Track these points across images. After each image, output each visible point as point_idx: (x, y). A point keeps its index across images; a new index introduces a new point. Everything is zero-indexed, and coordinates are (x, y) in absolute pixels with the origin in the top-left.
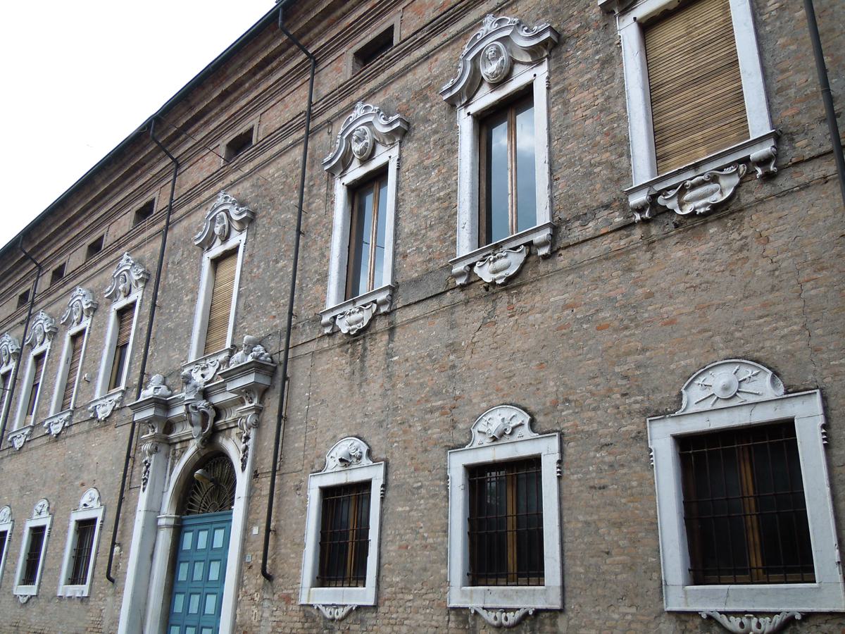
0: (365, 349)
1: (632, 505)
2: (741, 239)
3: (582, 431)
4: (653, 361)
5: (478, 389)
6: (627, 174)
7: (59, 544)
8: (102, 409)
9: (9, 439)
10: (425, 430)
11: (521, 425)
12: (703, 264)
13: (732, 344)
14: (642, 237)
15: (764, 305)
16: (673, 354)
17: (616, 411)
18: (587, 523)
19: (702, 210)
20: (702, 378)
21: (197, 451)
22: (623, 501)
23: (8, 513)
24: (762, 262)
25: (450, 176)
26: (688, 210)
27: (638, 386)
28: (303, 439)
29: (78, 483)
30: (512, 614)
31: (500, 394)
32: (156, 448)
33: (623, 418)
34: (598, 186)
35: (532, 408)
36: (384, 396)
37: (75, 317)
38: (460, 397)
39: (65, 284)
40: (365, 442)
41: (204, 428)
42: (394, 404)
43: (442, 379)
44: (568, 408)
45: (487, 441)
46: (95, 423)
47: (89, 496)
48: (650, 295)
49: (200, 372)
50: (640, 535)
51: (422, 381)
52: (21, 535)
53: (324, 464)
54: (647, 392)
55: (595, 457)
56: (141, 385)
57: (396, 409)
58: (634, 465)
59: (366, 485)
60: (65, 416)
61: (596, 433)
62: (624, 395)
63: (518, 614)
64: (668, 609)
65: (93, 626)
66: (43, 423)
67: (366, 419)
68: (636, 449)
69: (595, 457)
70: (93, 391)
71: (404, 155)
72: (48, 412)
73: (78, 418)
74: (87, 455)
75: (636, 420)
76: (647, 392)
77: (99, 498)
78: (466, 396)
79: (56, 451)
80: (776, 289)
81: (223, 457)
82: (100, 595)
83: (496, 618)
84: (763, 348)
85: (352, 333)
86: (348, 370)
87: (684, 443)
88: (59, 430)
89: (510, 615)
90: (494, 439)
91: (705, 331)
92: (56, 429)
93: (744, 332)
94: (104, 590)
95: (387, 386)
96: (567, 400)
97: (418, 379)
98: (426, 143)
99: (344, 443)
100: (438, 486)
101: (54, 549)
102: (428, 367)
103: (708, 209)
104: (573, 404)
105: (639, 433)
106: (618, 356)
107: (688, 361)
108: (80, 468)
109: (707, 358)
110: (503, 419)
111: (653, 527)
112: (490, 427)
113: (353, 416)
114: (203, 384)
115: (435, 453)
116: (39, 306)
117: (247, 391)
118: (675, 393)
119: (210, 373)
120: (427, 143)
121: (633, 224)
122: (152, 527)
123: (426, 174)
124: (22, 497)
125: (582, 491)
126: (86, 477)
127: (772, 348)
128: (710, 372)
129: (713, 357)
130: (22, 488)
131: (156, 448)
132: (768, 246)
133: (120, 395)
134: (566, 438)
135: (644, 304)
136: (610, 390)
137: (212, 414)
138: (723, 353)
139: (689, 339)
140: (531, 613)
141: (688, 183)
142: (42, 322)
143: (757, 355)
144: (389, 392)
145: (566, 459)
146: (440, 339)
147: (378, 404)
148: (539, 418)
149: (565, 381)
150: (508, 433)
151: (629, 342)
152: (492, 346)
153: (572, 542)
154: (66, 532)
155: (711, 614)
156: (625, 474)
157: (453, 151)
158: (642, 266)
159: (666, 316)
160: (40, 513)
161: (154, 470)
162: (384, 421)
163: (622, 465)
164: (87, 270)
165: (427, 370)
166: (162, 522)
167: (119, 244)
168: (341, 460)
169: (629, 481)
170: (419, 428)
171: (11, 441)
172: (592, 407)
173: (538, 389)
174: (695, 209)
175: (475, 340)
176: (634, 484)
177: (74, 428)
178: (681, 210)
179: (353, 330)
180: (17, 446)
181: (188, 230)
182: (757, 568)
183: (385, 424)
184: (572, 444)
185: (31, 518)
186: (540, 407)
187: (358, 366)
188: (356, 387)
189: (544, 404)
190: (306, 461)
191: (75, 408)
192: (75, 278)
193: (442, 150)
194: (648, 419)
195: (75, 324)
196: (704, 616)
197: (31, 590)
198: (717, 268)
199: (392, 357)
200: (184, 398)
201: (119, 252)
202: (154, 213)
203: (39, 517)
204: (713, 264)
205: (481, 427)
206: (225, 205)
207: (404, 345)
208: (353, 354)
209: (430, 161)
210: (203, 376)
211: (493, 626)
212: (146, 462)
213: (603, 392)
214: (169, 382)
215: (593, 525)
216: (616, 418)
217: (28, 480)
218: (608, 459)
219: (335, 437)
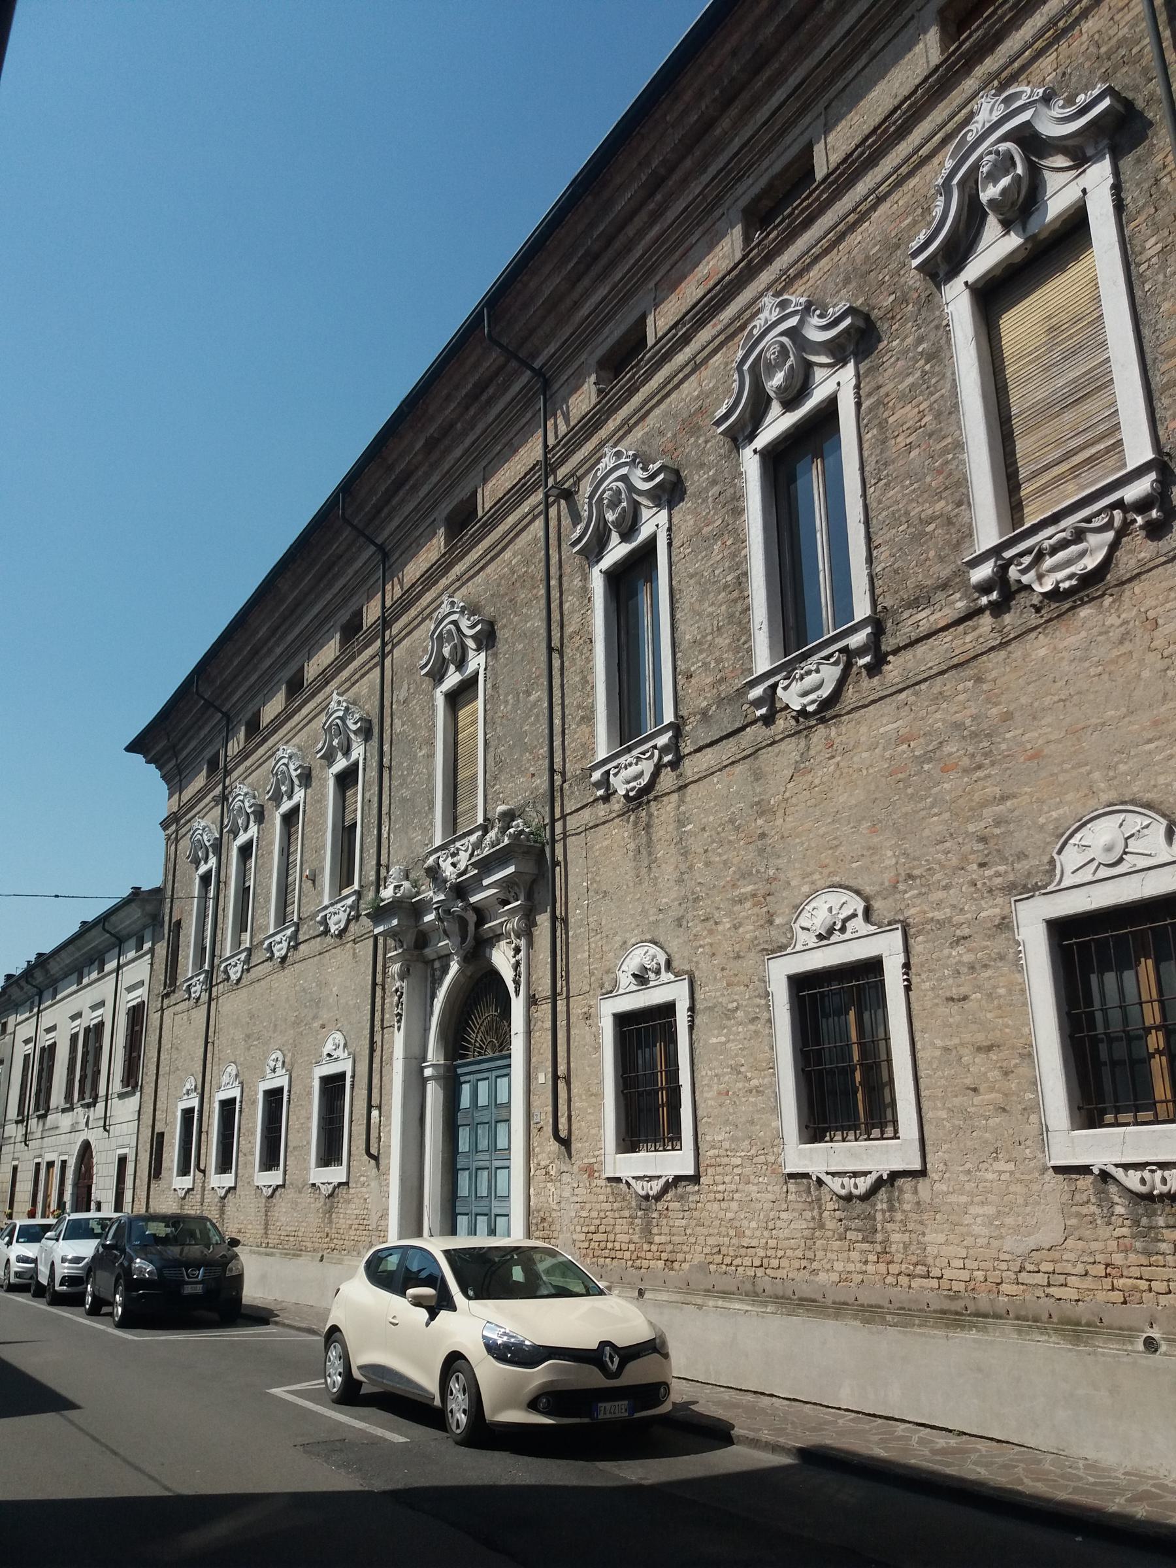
0: (650, 815)
1: (1000, 1021)
2: (1121, 625)
3: (932, 919)
4: (1016, 813)
5: (797, 865)
6: (968, 534)
7: (303, 1112)
8: (335, 919)
9: (222, 968)
10: (736, 927)
11: (854, 915)
12: (1074, 665)
13: (1115, 782)
14: (993, 629)
15: (1156, 723)
16: (1041, 801)
17: (973, 889)
18: (947, 1049)
19: (1066, 585)
20: (1078, 836)
21: (461, 971)
22: (989, 1015)
23: (234, 1073)
24: (1152, 657)
25: (740, 551)
26: (1048, 586)
27: (998, 851)
28: (586, 948)
29: (316, 1025)
30: (863, 1178)
31: (826, 871)
32: (408, 970)
33: (983, 898)
34: (932, 554)
35: (868, 890)
36: (680, 881)
37: (284, 789)
38: (775, 879)
39: (265, 740)
40: (662, 948)
41: (464, 939)
42: (693, 893)
43: (751, 855)
44: (911, 888)
45: (812, 941)
46: (328, 939)
47: (332, 1042)
48: (1008, 717)
49: (450, 860)
50: (1013, 1062)
51: (725, 857)
52: (254, 1102)
53: (616, 983)
54: (1011, 859)
55: (950, 956)
56: (379, 883)
57: (697, 900)
58: (1000, 964)
59: (669, 1009)
60: (289, 932)
61: (950, 922)
62: (982, 865)
63: (870, 1179)
64: (1054, 1163)
65: (357, 1221)
66: (262, 943)
67: (661, 916)
68: (999, 944)
69: (950, 956)
70: (320, 894)
71: (675, 520)
72: (267, 927)
73: (305, 933)
74: (322, 985)
75: (999, 901)
76: (1011, 859)
77: (345, 1046)
78: (782, 876)
79: (284, 979)
80: (1169, 697)
81: (494, 976)
82: (362, 1179)
83: (843, 1186)
84: (1155, 786)
85: (631, 794)
86: (632, 846)
87: (1062, 931)
88: (283, 952)
89: (860, 1181)
90: (820, 937)
91: (1080, 765)
92: (279, 951)
93: (1131, 764)
94: (366, 1171)
95: (683, 868)
96: (910, 876)
97: (720, 855)
98: (703, 501)
99: (637, 952)
100: (758, 1006)
101: (298, 1119)
102: (731, 838)
103: (1074, 582)
104: (918, 881)
105: (1004, 918)
106: (971, 809)
107: (1061, 811)
108: (317, 1003)
109: (1084, 805)
110: (830, 910)
111: (1028, 1055)
112: (815, 921)
113: (644, 912)
114: (454, 876)
115: (752, 959)
116: (235, 774)
117: (507, 884)
118: (1046, 859)
119: (463, 859)
120: (705, 501)
121: (980, 611)
122: (416, 1082)
123: (706, 549)
124: (249, 1049)
125: (937, 1004)
126: (325, 1015)
127: (1167, 785)
128: (1089, 826)
129: (1092, 803)
130: (248, 1036)
131: (408, 970)
132: (1156, 633)
133: (354, 898)
134: (912, 931)
135: (1001, 730)
136: (964, 858)
137: (472, 918)
138: (1105, 797)
139: (1061, 779)
140: (885, 1177)
141: (1046, 544)
142: (241, 798)
143: (1148, 796)
144: (686, 877)
145: (914, 961)
146: (743, 797)
147: (673, 895)
148: (877, 904)
149: (905, 849)
150: (837, 927)
151: (984, 788)
152: (809, 803)
153: (929, 1076)
154: (310, 1093)
155: (1104, 1167)
156: (989, 978)
157: (738, 512)
158: (994, 674)
159: (1029, 746)
160: (274, 1070)
161: (408, 1000)
162: (683, 917)
163: (986, 966)
164: (289, 717)
165: (730, 842)
166: (428, 1072)
167: (326, 677)
168: (634, 975)
169: (995, 987)
170: (728, 926)
171: (226, 972)
172: (943, 883)
173: (872, 862)
174: (1058, 583)
175: (787, 795)
176: (1002, 991)
177: (302, 947)
178: (1041, 584)
179: (632, 789)
180: (234, 977)
181: (411, 652)
182: (1167, 1102)
183: (684, 923)
184: (920, 939)
185: (263, 1079)
186: (877, 888)
187: (644, 841)
188: (644, 871)
189: (882, 884)
190: (593, 979)
191: (300, 919)
192: (275, 731)
193: (725, 510)
194: (1013, 899)
195: (285, 798)
196: (1096, 1171)
197: (274, 1178)
198: (1093, 671)
199: (685, 826)
200: (432, 898)
201: (328, 689)
202: (365, 628)
203: (273, 1075)
204: (1087, 664)
205: (804, 921)
206: (449, 608)
207: (698, 808)
208: (636, 824)
209: (710, 528)
210: (454, 865)
211: (840, 1197)
212: (397, 990)
213: (955, 861)
214: (412, 876)
215: (954, 1052)
216: (972, 898)
217: (255, 1024)
218: (967, 958)
219: (625, 943)
